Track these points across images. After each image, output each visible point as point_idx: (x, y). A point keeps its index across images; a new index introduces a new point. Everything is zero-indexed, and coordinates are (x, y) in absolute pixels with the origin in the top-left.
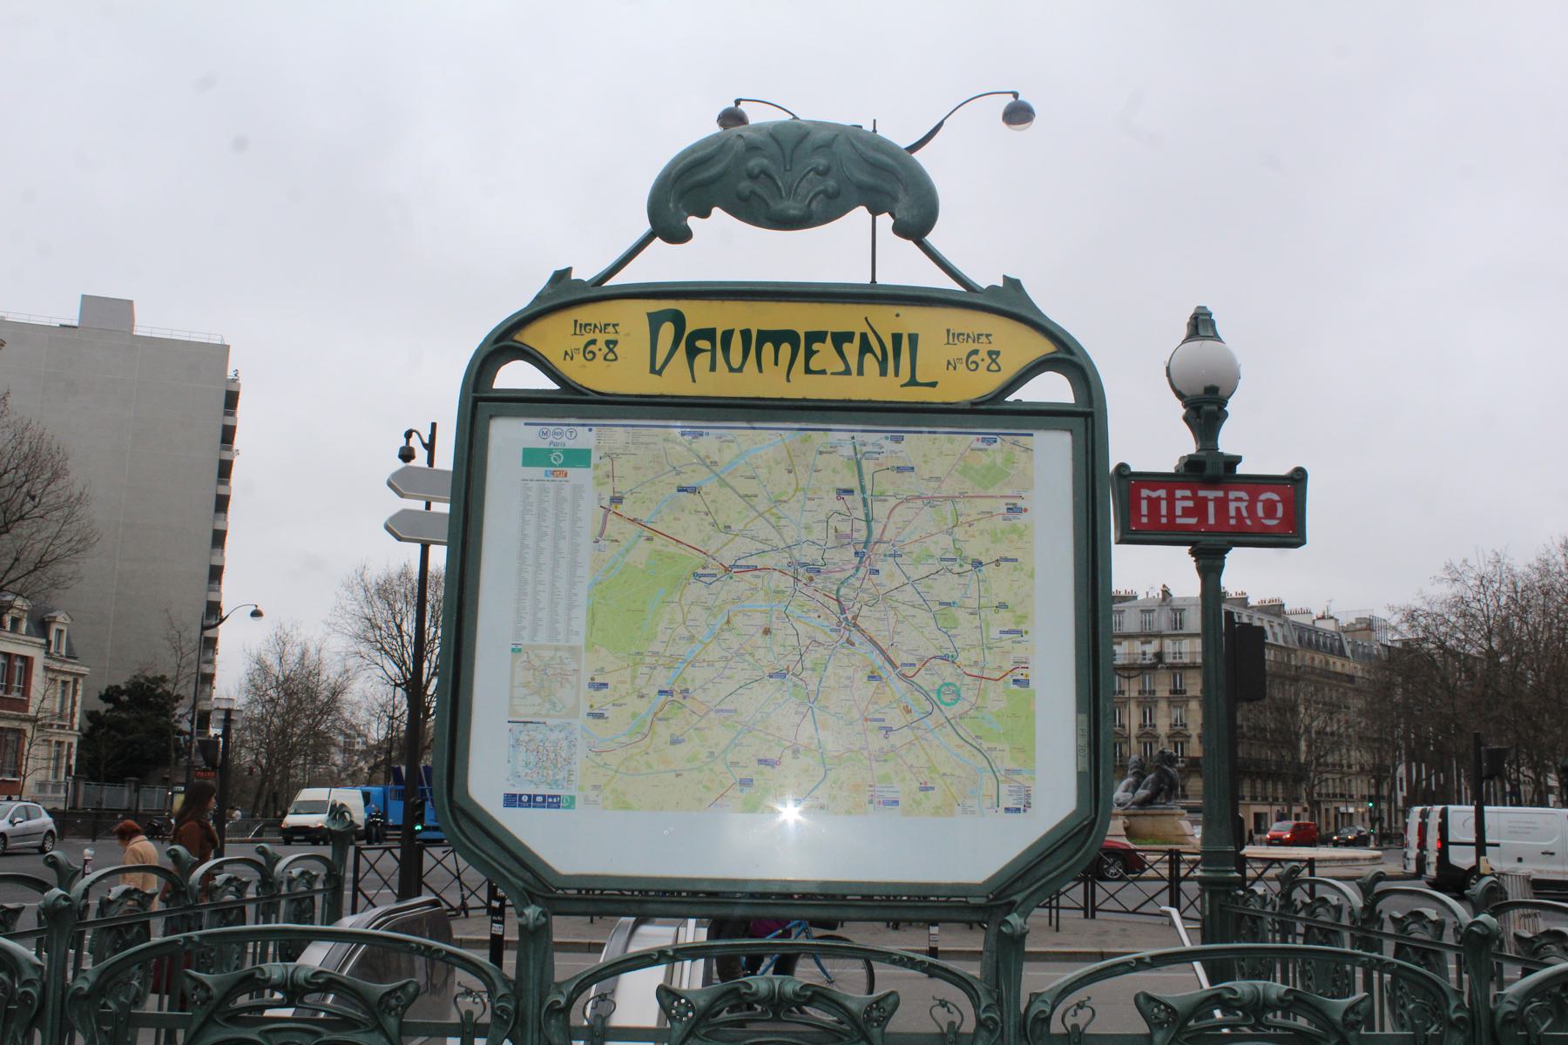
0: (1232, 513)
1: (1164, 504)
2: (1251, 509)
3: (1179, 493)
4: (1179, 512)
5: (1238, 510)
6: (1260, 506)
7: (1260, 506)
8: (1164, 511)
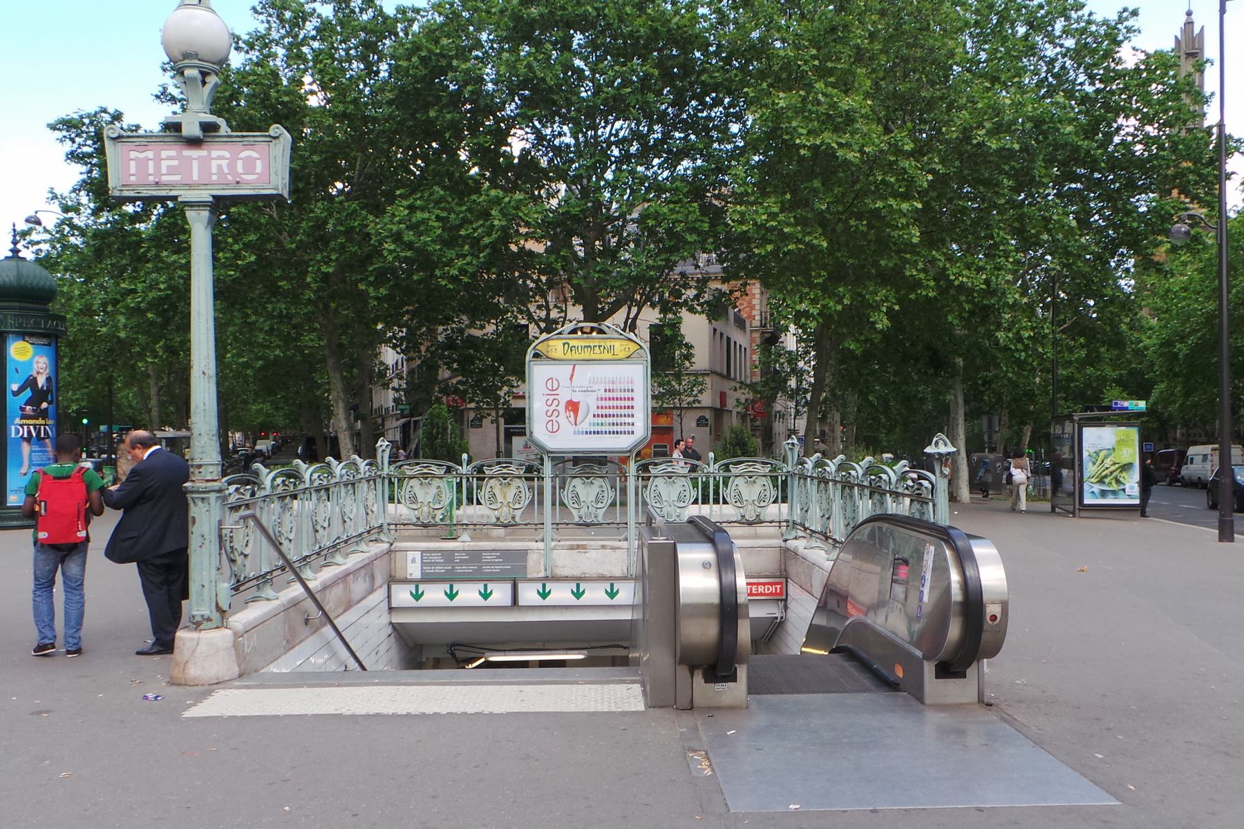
0: (214, 170)
1: (151, 164)
2: (232, 166)
3: (164, 154)
4: (164, 170)
5: (220, 167)
6: (240, 163)
7: (240, 163)
8: (151, 171)
